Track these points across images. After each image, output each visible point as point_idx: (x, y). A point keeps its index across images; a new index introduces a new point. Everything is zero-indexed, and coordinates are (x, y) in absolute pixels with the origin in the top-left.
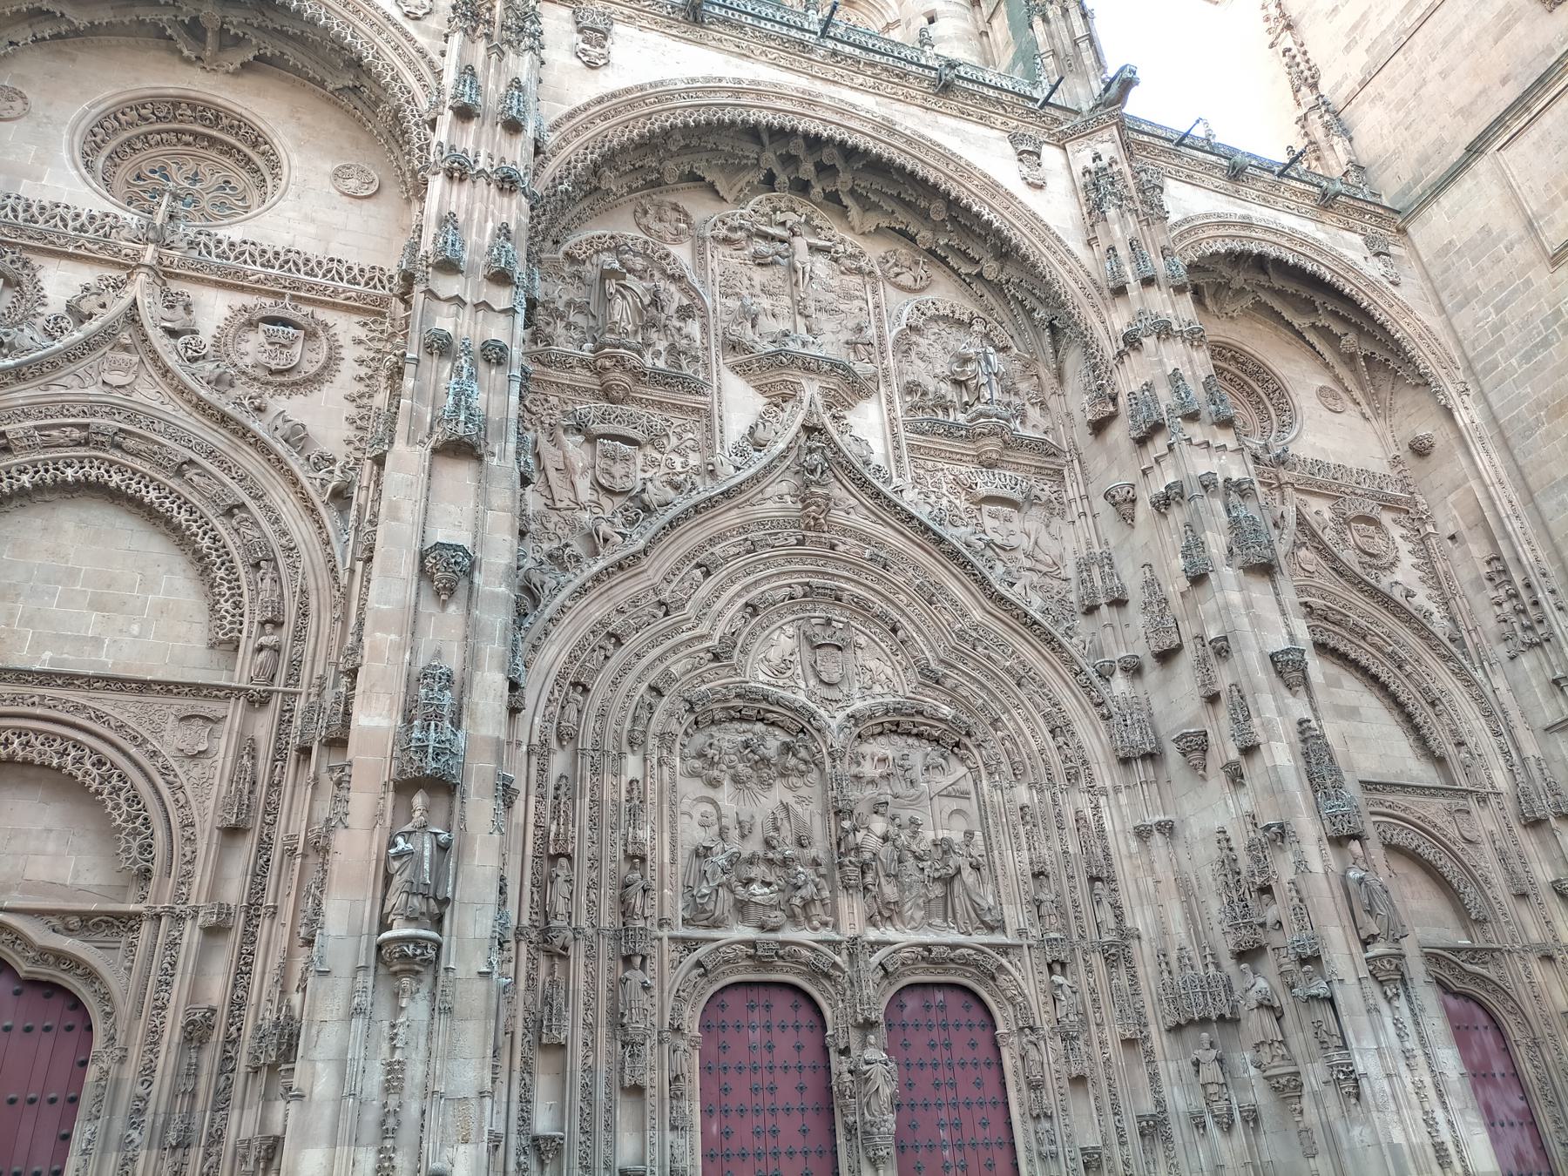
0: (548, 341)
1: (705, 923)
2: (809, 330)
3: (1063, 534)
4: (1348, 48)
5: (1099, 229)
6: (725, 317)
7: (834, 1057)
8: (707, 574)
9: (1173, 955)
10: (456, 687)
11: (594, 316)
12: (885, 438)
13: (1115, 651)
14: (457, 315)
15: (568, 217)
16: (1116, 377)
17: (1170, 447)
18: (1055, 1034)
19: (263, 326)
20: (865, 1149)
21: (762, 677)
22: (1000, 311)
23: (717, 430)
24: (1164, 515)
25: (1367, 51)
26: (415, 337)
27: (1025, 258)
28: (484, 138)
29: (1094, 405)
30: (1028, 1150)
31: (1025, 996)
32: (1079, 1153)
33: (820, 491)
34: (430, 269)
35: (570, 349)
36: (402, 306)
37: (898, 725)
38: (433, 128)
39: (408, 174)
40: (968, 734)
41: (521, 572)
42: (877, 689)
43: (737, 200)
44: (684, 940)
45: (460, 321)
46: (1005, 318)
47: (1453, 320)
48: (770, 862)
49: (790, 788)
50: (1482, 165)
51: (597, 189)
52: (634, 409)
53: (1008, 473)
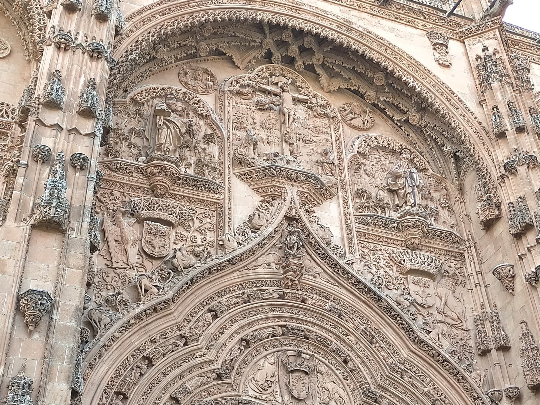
0: (116, 154)
2: (292, 153)
3: (465, 298)
5: (487, 94)
6: (235, 143)
8: (216, 317)
10: (34, 393)
11: (147, 139)
12: (342, 226)
13: (502, 383)
14: (56, 137)
15: (135, 75)
16: (500, 192)
22: (420, 145)
23: (227, 218)
24: (535, 288)
26: (26, 150)
27: (437, 111)
28: (82, 24)
29: (485, 210)
34: (40, 106)
35: (131, 160)
36: (20, 129)
38: (49, 17)
39: (30, 45)
41: (86, 312)
43: (247, 68)
45: (58, 141)
46: (424, 150)
51: (154, 58)
52: (171, 201)
53: (426, 254)
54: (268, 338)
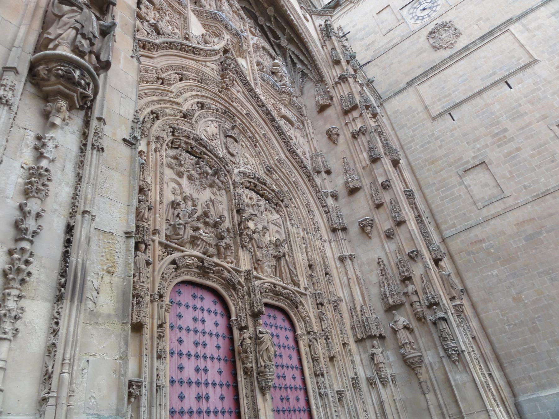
1: (176, 241)
7: (236, 333)
8: (181, 80)
9: (358, 308)
17: (361, 115)
18: (322, 336)
20: (259, 382)
21: (203, 137)
30: (314, 392)
31: (309, 317)
32: (336, 393)
33: (232, 74)
37: (255, 186)
40: (282, 201)
42: (249, 167)
44: (166, 246)
47: (398, 133)
48: (206, 224)
49: (213, 194)
50: (411, 89)
54: (213, 110)
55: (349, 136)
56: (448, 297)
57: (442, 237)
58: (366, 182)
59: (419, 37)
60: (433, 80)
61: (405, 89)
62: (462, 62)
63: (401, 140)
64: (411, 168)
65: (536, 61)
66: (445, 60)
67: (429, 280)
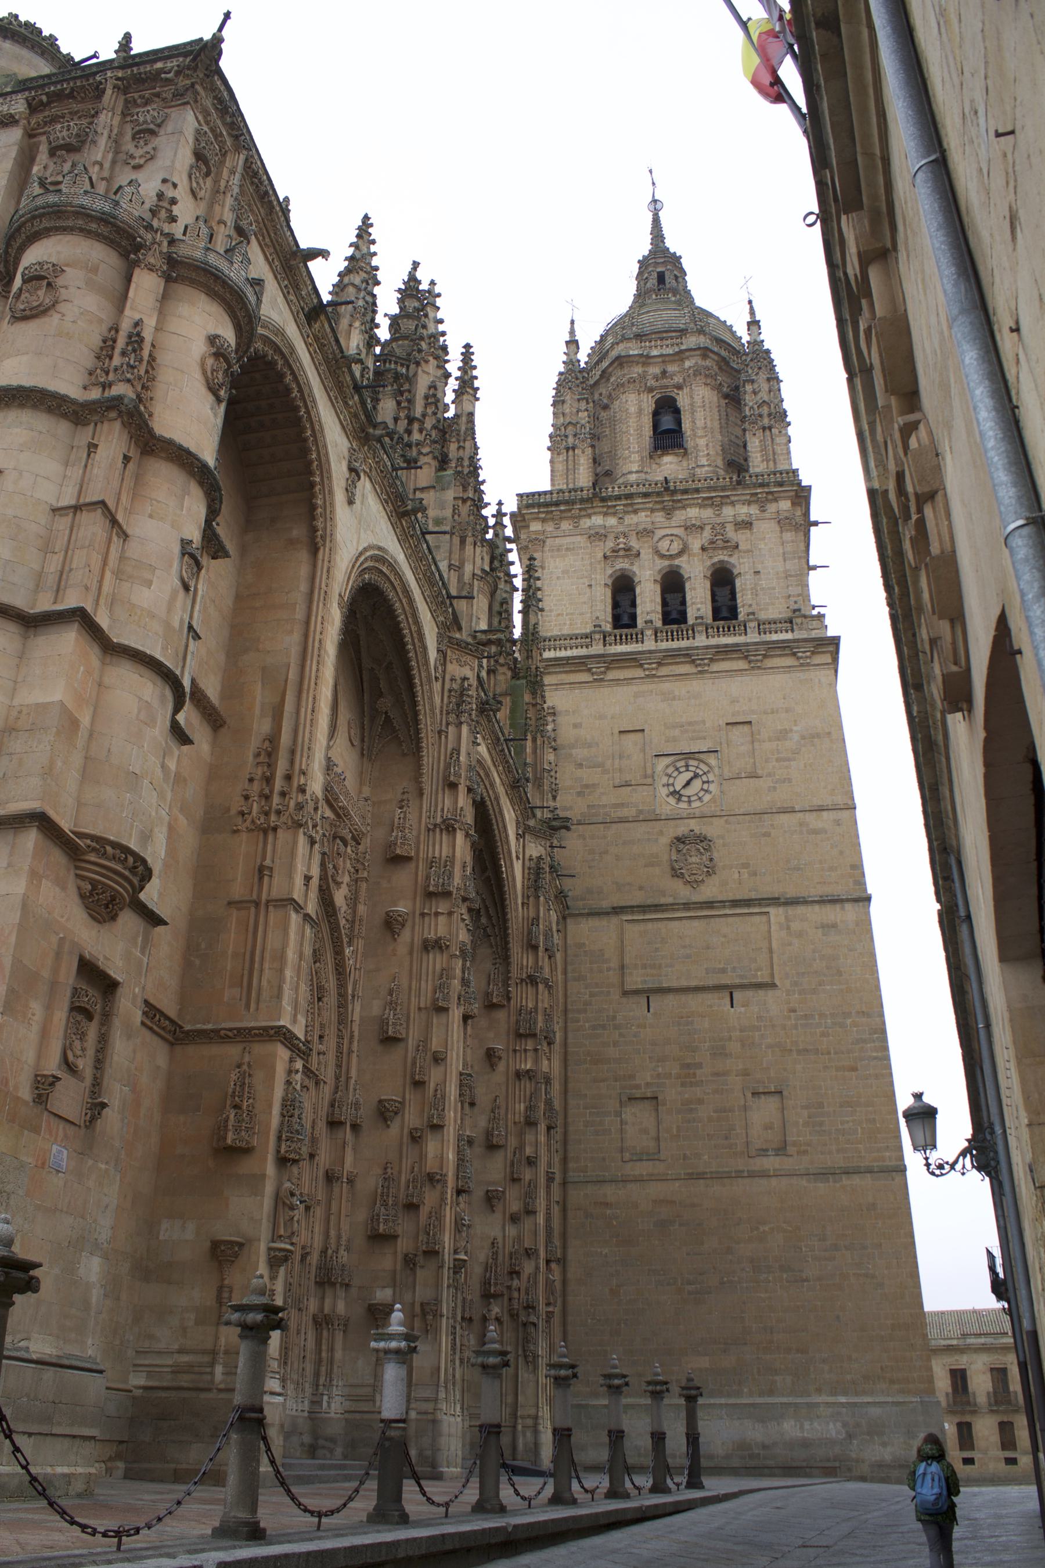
4: (579, 794)
17: (536, 1050)
19: (338, 841)
25: (588, 806)
47: (569, 984)
50: (614, 920)
55: (512, 1070)
56: (545, 1301)
57: (564, 1178)
58: (513, 1142)
59: (661, 833)
60: (650, 925)
61: (607, 914)
62: (696, 923)
63: (569, 1000)
64: (566, 1053)
65: (773, 986)
66: (678, 904)
67: (535, 1283)
